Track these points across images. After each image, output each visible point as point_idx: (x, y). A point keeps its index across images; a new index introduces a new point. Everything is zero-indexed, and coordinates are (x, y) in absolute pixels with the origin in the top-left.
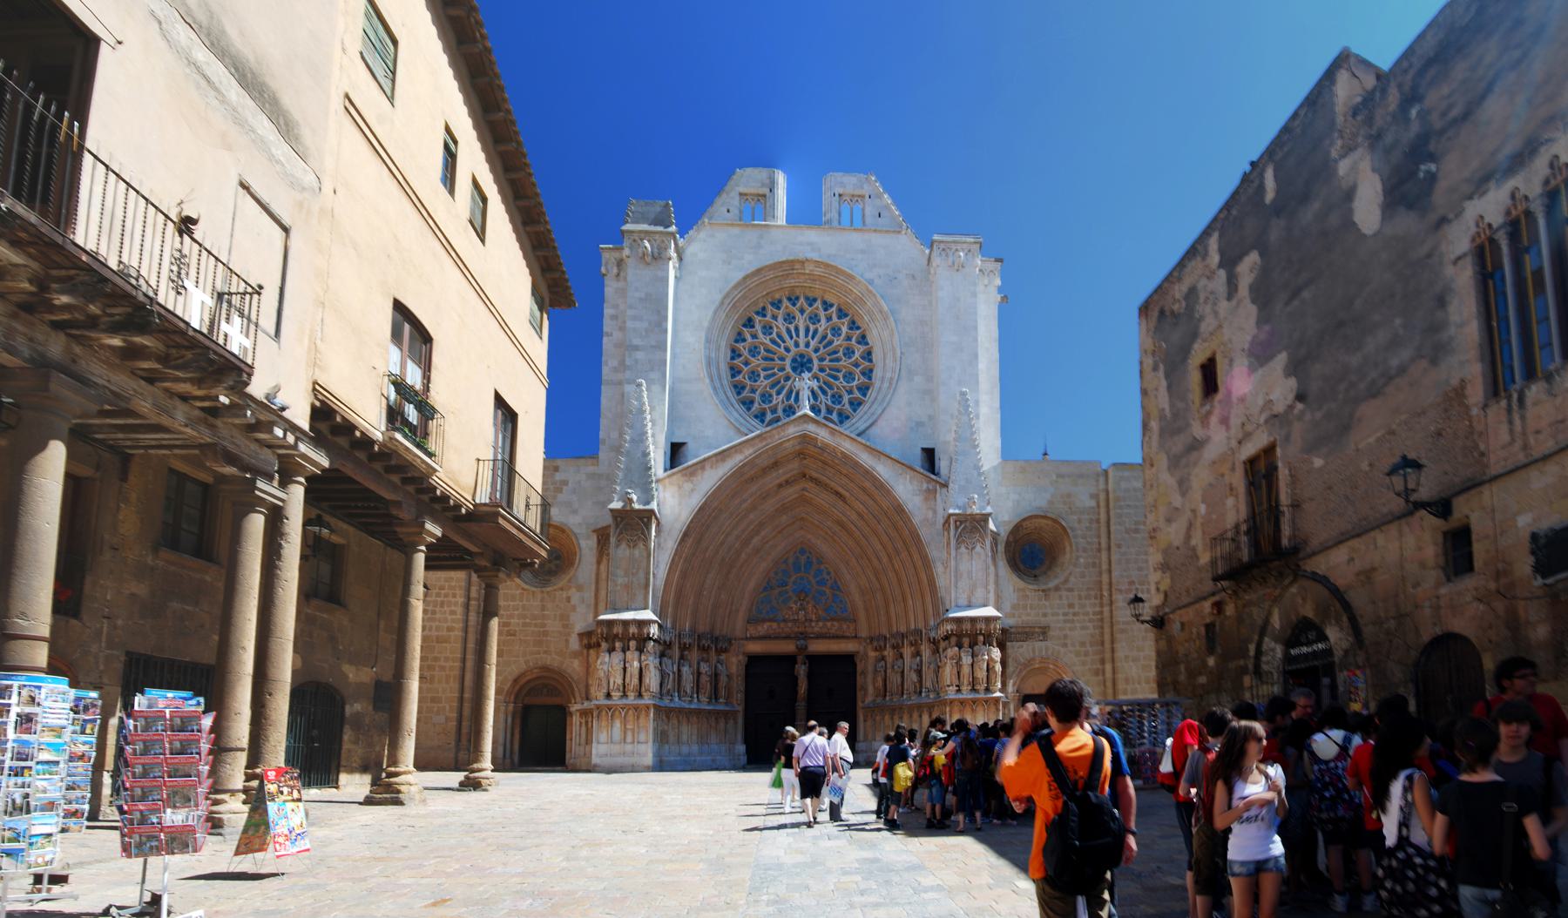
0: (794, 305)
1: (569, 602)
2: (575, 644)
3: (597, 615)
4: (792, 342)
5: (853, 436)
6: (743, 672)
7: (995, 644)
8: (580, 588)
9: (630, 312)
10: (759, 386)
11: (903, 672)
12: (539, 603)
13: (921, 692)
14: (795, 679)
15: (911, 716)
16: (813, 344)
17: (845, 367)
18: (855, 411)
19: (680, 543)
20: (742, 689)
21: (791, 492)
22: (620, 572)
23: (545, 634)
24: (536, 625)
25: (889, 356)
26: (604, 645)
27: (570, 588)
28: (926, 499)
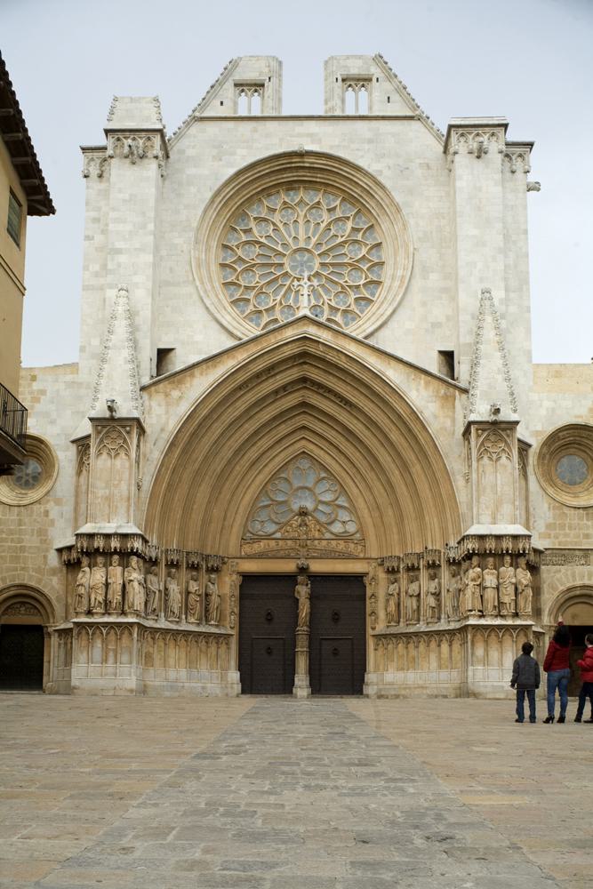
0: (293, 200)
1: (47, 516)
2: (54, 560)
3: (76, 527)
4: (290, 240)
5: (360, 337)
6: (237, 593)
7: (524, 566)
8: (58, 502)
9: (112, 215)
10: (254, 288)
11: (419, 595)
12: (15, 517)
13: (439, 619)
15: (428, 646)
16: (314, 240)
17: (350, 265)
18: (362, 312)
19: (166, 454)
20: (236, 610)
22: (100, 484)
23: (23, 549)
24: (12, 541)
25: (401, 252)
26: (85, 561)
27: (48, 501)
28: (443, 407)
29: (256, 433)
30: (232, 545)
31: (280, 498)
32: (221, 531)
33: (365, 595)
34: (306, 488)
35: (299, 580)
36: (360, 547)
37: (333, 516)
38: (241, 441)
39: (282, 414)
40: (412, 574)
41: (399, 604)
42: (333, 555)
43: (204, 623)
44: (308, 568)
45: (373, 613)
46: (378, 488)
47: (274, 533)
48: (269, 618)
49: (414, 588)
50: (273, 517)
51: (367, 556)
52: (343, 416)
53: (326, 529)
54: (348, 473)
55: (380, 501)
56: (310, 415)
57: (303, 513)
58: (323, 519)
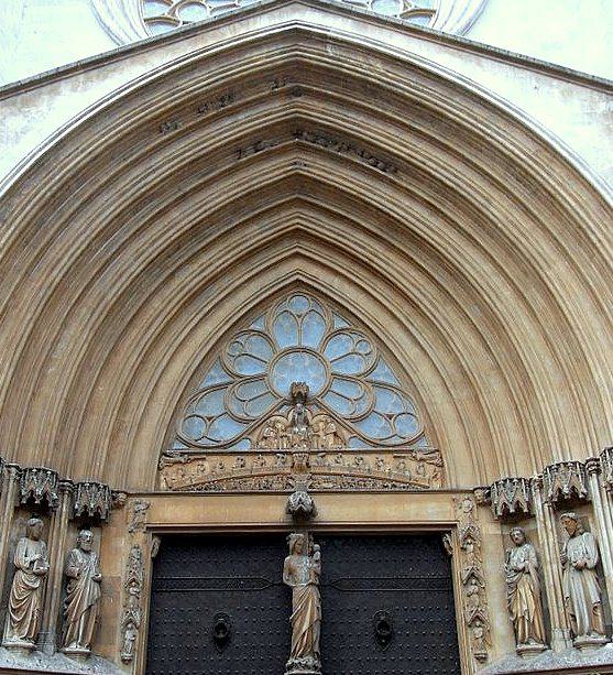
14: (288, 591)
20: (140, 617)
21: (269, 172)
29: (195, 230)
30: (138, 464)
31: (248, 370)
32: (113, 437)
33: (451, 579)
34: (305, 350)
35: (292, 543)
36: (430, 469)
37: (364, 407)
38: (161, 244)
39: (252, 196)
40: (572, 515)
41: (541, 597)
42: (369, 487)
43: (51, 648)
44: (312, 513)
45: (477, 619)
46: (463, 338)
47: (233, 443)
48: (222, 639)
49: (580, 548)
50: (234, 408)
51: (448, 487)
52: (380, 195)
53: (350, 430)
54: (394, 317)
55: (468, 361)
56: (313, 207)
57: (299, 397)
58: (343, 410)
